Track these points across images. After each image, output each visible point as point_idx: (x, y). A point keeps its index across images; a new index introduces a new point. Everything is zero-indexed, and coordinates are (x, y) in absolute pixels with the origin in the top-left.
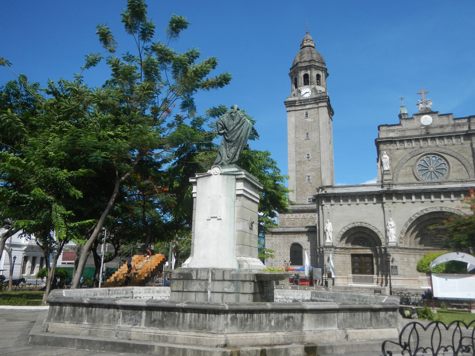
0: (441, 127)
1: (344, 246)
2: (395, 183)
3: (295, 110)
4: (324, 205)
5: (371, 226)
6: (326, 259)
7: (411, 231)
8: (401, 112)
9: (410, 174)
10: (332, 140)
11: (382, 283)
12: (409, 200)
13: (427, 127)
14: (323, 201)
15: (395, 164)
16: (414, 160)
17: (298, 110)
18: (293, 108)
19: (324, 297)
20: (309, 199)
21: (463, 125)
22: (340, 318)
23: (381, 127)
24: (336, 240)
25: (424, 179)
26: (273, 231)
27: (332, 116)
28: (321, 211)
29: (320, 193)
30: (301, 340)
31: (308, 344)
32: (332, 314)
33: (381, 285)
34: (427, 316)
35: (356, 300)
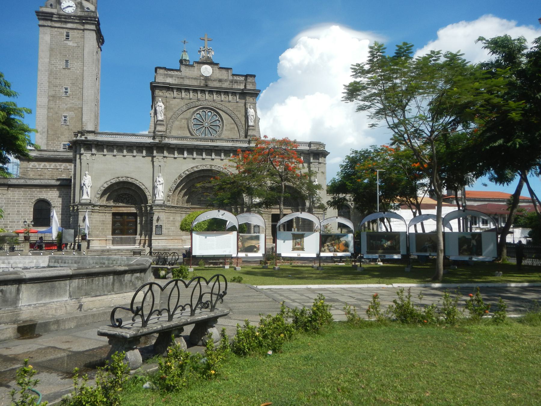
0: (220, 81)
1: (105, 203)
2: (168, 134)
3: (51, 27)
4: (83, 154)
5: (137, 182)
6: (81, 218)
7: (179, 189)
8: (182, 57)
9: (185, 127)
10: (99, 76)
11: (145, 243)
12: (181, 156)
13: (207, 79)
14: (82, 149)
15: (170, 115)
16: (190, 112)
17: (56, 27)
18: (49, 23)
19: (65, 263)
20: (64, 145)
21: (240, 83)
22: (74, 286)
23: (158, 70)
24: (95, 196)
25: (197, 134)
26: (9, 183)
27: (102, 45)
28: (78, 161)
29: (79, 138)
30: (14, 319)
31: (24, 322)
32: (62, 282)
33: (144, 246)
34: (182, 275)
35: (104, 264)
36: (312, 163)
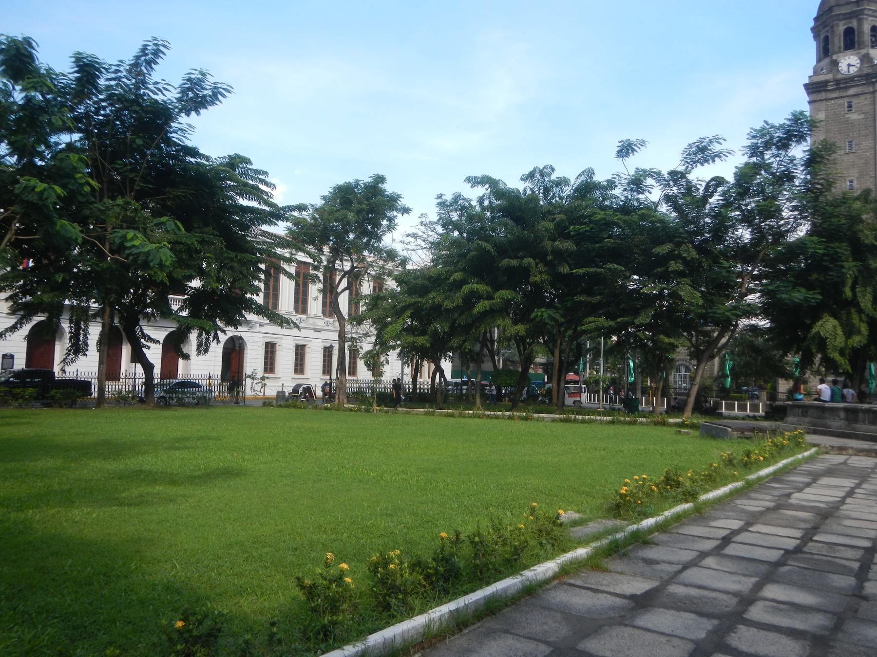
17: (832, 99)
18: (823, 95)
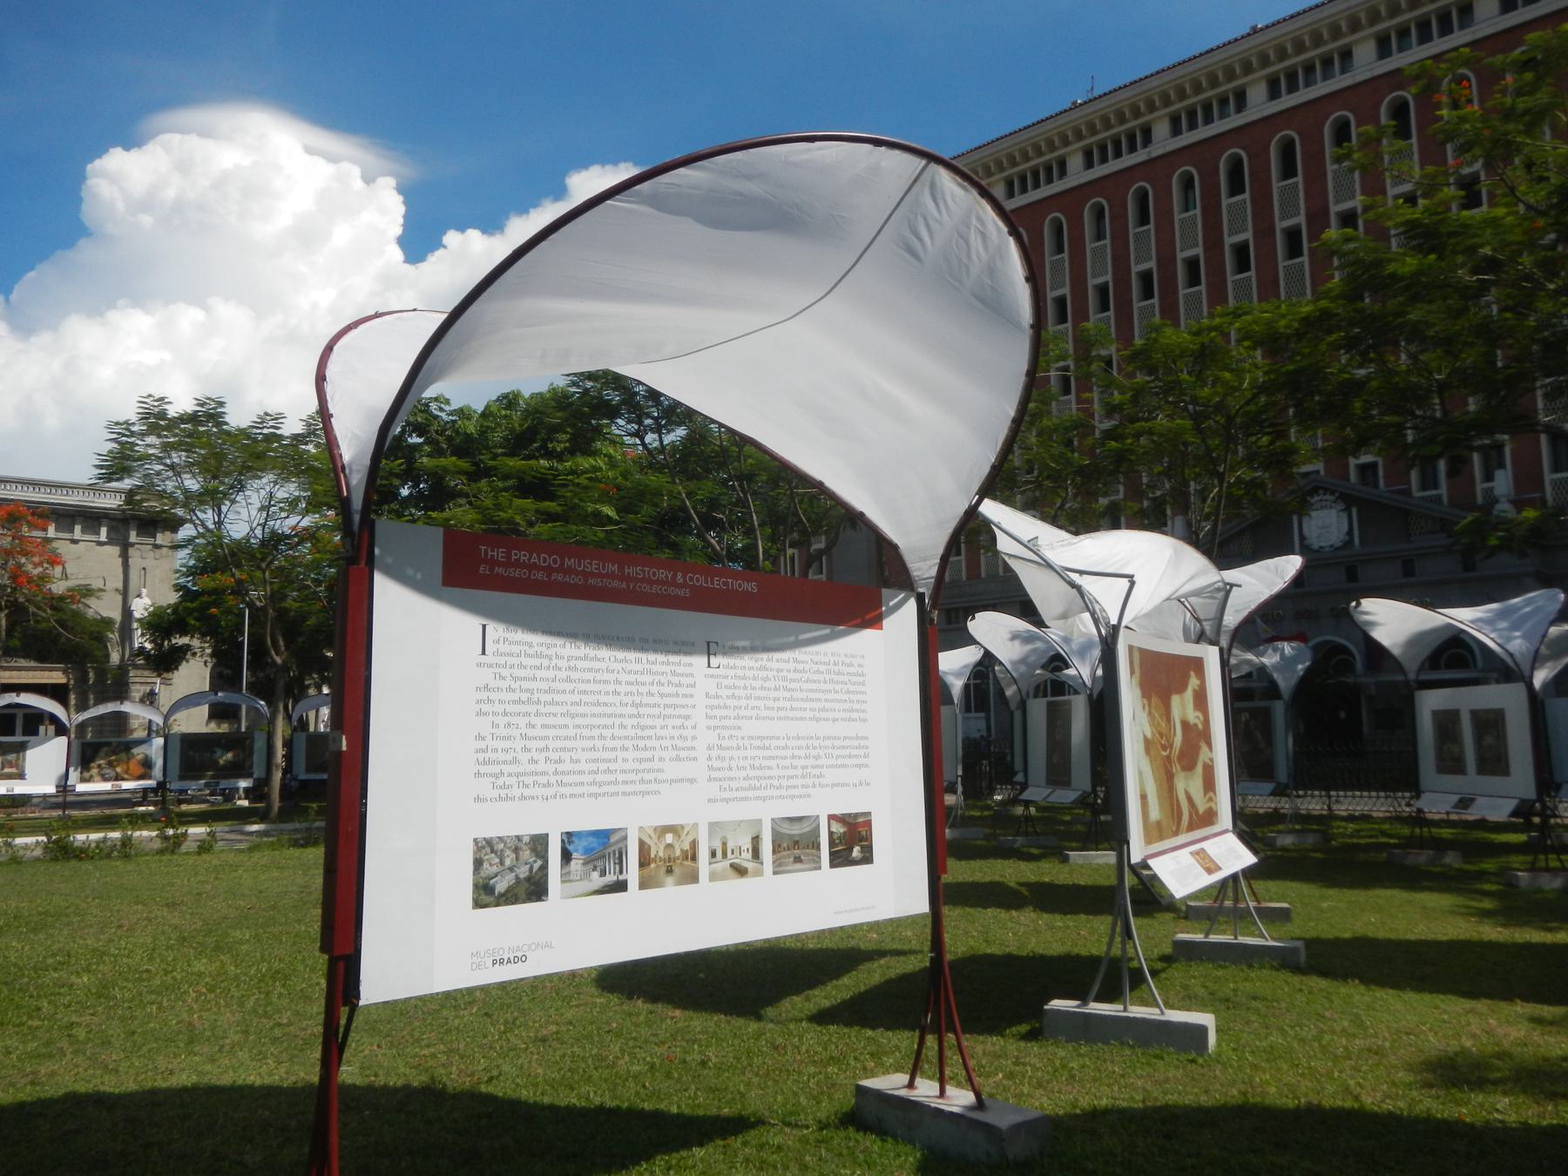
36: (133, 545)
